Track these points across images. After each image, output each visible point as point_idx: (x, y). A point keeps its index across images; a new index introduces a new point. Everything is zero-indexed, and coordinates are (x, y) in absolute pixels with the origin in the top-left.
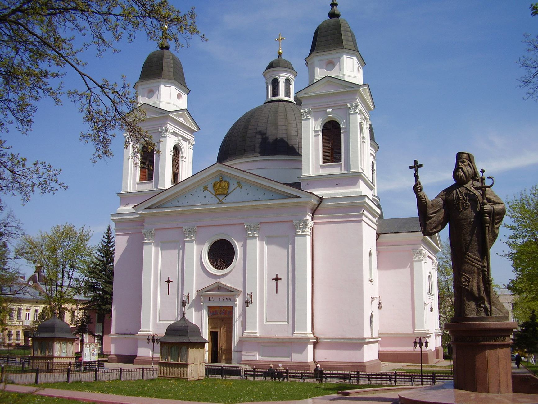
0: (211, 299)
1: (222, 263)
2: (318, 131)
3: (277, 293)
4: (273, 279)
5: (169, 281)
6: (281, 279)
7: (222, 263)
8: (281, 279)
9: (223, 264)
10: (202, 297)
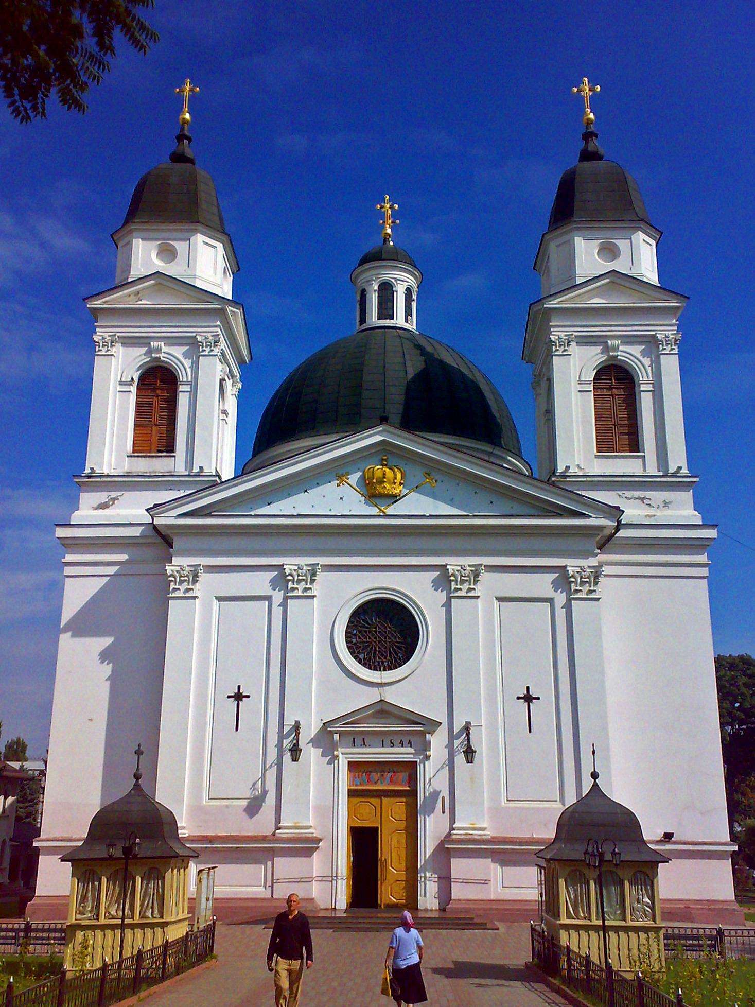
0: (358, 741)
1: (382, 655)
2: (588, 383)
3: (530, 731)
4: (519, 698)
5: (238, 697)
6: (538, 698)
7: (382, 655)
8: (538, 698)
9: (386, 658)
10: (336, 737)
